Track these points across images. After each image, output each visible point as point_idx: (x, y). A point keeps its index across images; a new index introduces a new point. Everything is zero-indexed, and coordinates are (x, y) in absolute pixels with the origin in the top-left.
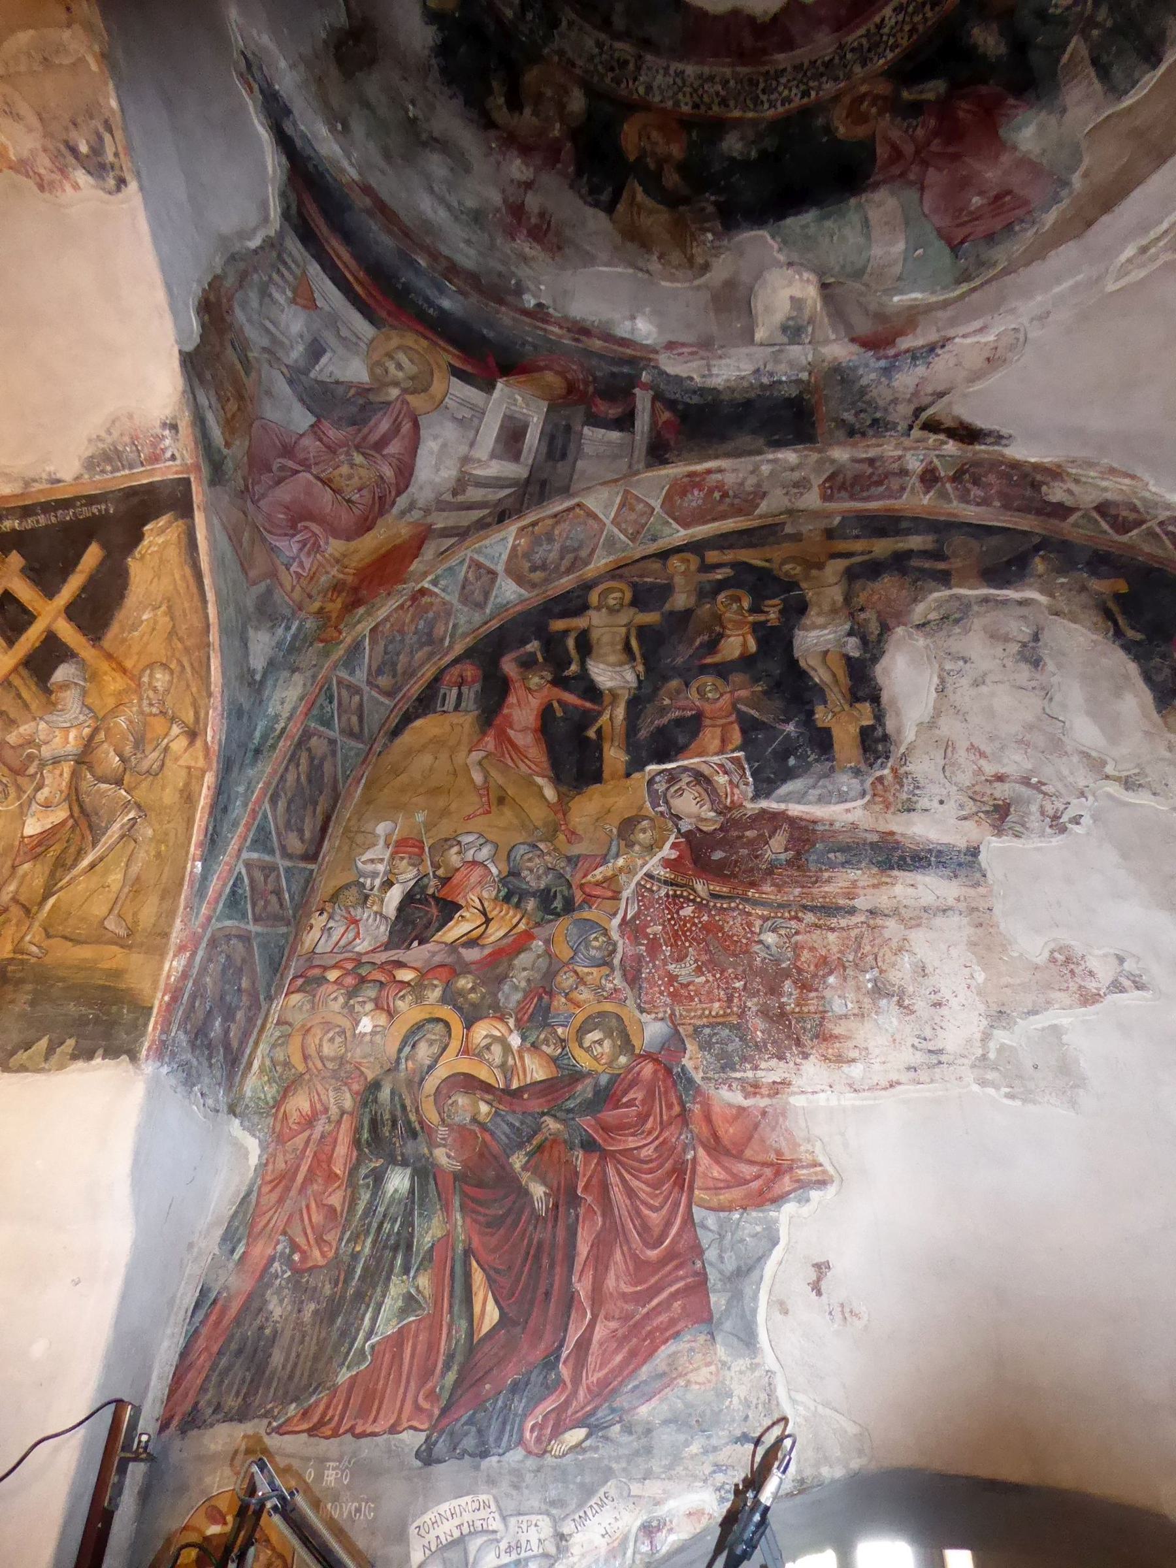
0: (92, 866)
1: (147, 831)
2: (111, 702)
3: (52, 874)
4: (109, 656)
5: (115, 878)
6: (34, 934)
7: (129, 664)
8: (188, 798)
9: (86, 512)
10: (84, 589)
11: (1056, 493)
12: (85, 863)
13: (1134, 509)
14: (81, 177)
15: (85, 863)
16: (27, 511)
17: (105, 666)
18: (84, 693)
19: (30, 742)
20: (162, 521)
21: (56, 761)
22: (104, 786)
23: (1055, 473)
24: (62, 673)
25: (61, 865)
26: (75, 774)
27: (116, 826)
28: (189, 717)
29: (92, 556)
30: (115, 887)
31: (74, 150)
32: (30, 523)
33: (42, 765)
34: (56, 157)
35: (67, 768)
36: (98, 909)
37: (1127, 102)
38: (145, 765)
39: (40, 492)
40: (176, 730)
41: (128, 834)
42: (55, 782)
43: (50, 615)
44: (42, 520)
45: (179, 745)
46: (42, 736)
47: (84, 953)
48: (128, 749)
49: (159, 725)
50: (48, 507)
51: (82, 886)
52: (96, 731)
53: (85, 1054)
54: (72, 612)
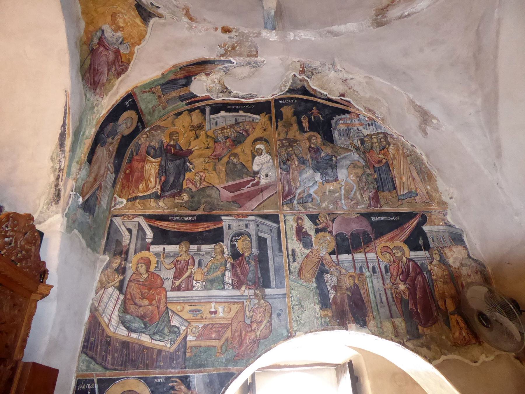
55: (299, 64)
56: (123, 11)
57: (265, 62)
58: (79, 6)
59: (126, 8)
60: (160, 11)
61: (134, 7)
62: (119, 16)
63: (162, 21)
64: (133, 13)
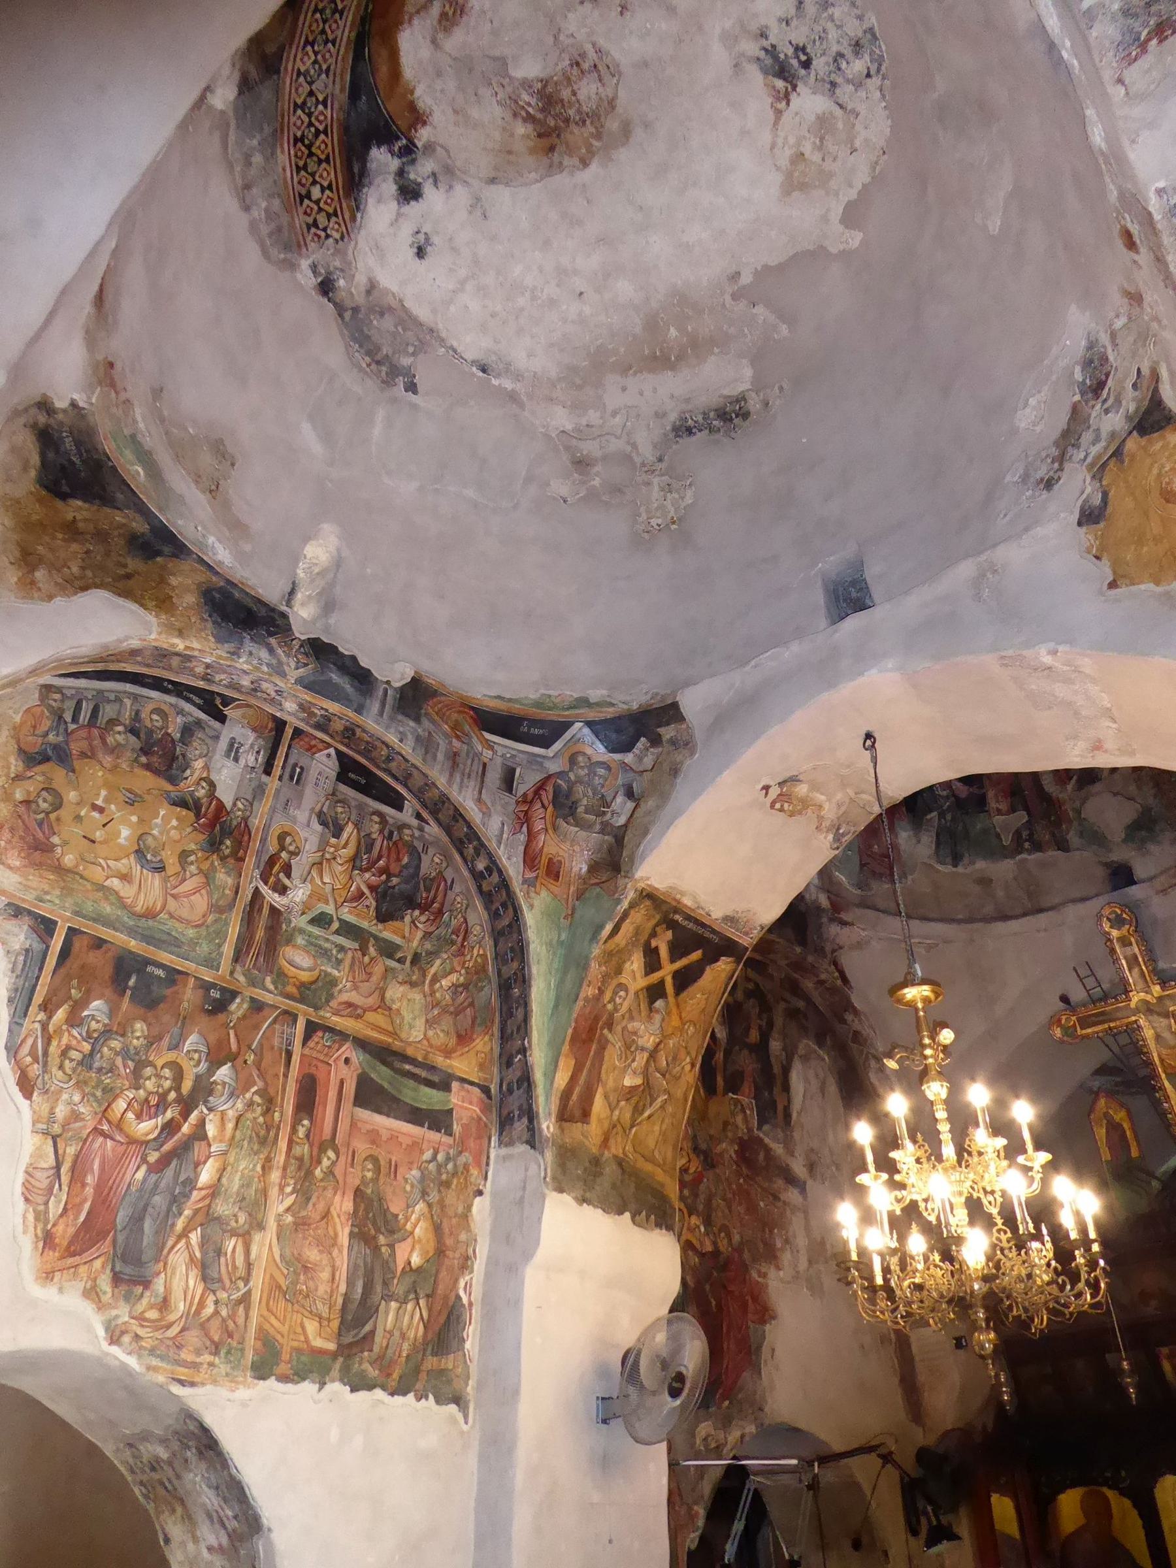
0: (649, 1117)
1: (670, 1109)
2: (670, 1031)
3: (633, 1114)
4: (678, 1006)
5: (657, 1128)
6: (629, 1148)
7: (683, 1015)
8: (686, 1100)
9: (707, 934)
10: (685, 967)
11: (849, 1017)
12: (646, 1114)
13: (866, 1040)
14: (831, 837)
15: (646, 1114)
16: (689, 918)
17: (674, 1010)
18: (663, 1020)
19: (635, 1033)
20: (730, 959)
21: (643, 1049)
22: (658, 1075)
23: (856, 1012)
24: (659, 1004)
25: (637, 1110)
26: (648, 1061)
27: (660, 1100)
28: (694, 1055)
29: (696, 955)
30: (657, 1133)
31: (838, 829)
32: (685, 923)
33: (636, 1049)
34: (833, 826)
35: (646, 1055)
36: (651, 1143)
37: (940, 867)
38: (675, 1071)
39: (700, 914)
40: (688, 1060)
41: (662, 1107)
42: (641, 1059)
43: (667, 970)
44: (691, 925)
45: (688, 1068)
46: (641, 1033)
47: (649, 1167)
48: (670, 1059)
49: (683, 1051)
50: (697, 922)
51: (645, 1126)
52: (661, 1042)
53: (658, 1225)
54: (676, 975)
55: (1133, 74)
56: (1155, 471)
57: (1161, 184)
58: (1143, 587)
59: (1148, 461)
60: (1146, 371)
61: (1143, 441)
62: (1168, 483)
63: (1164, 373)
64: (1158, 446)
